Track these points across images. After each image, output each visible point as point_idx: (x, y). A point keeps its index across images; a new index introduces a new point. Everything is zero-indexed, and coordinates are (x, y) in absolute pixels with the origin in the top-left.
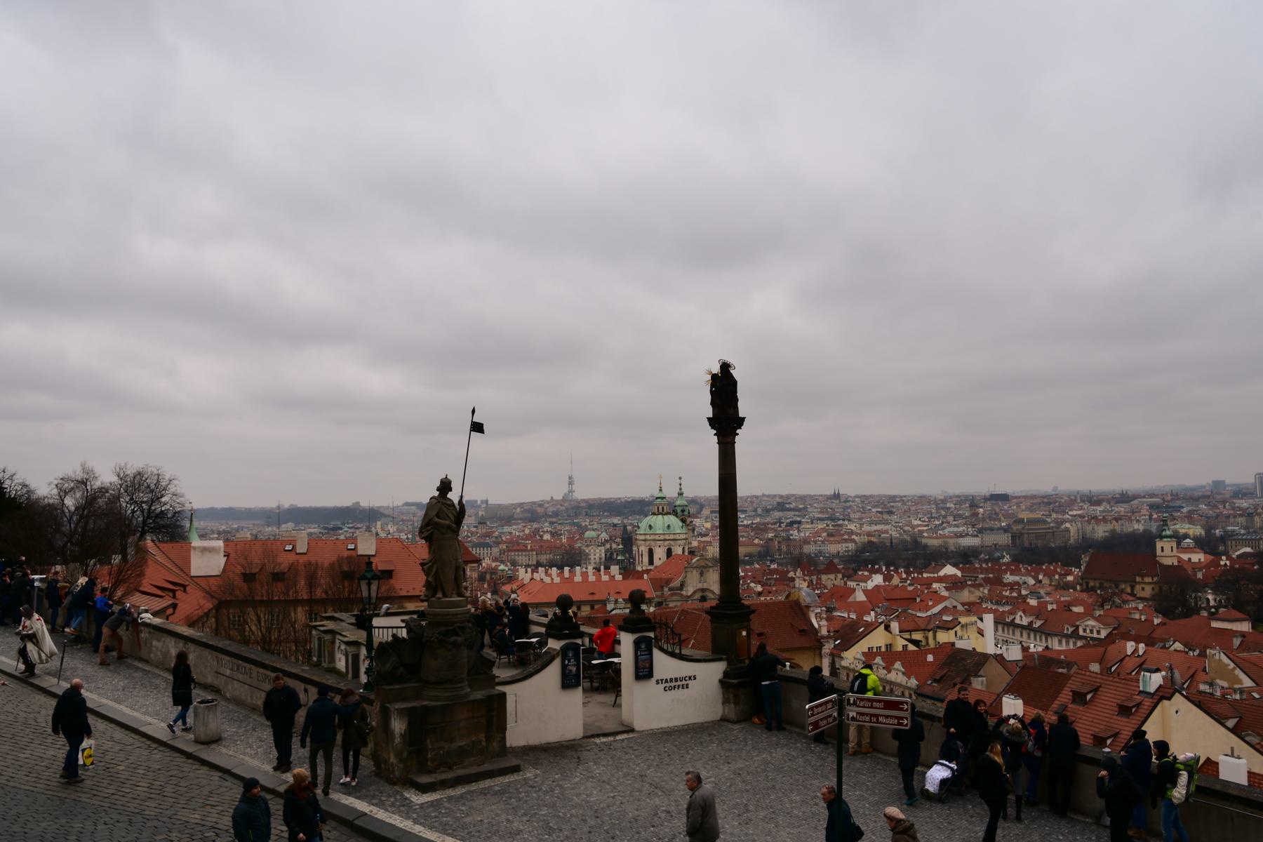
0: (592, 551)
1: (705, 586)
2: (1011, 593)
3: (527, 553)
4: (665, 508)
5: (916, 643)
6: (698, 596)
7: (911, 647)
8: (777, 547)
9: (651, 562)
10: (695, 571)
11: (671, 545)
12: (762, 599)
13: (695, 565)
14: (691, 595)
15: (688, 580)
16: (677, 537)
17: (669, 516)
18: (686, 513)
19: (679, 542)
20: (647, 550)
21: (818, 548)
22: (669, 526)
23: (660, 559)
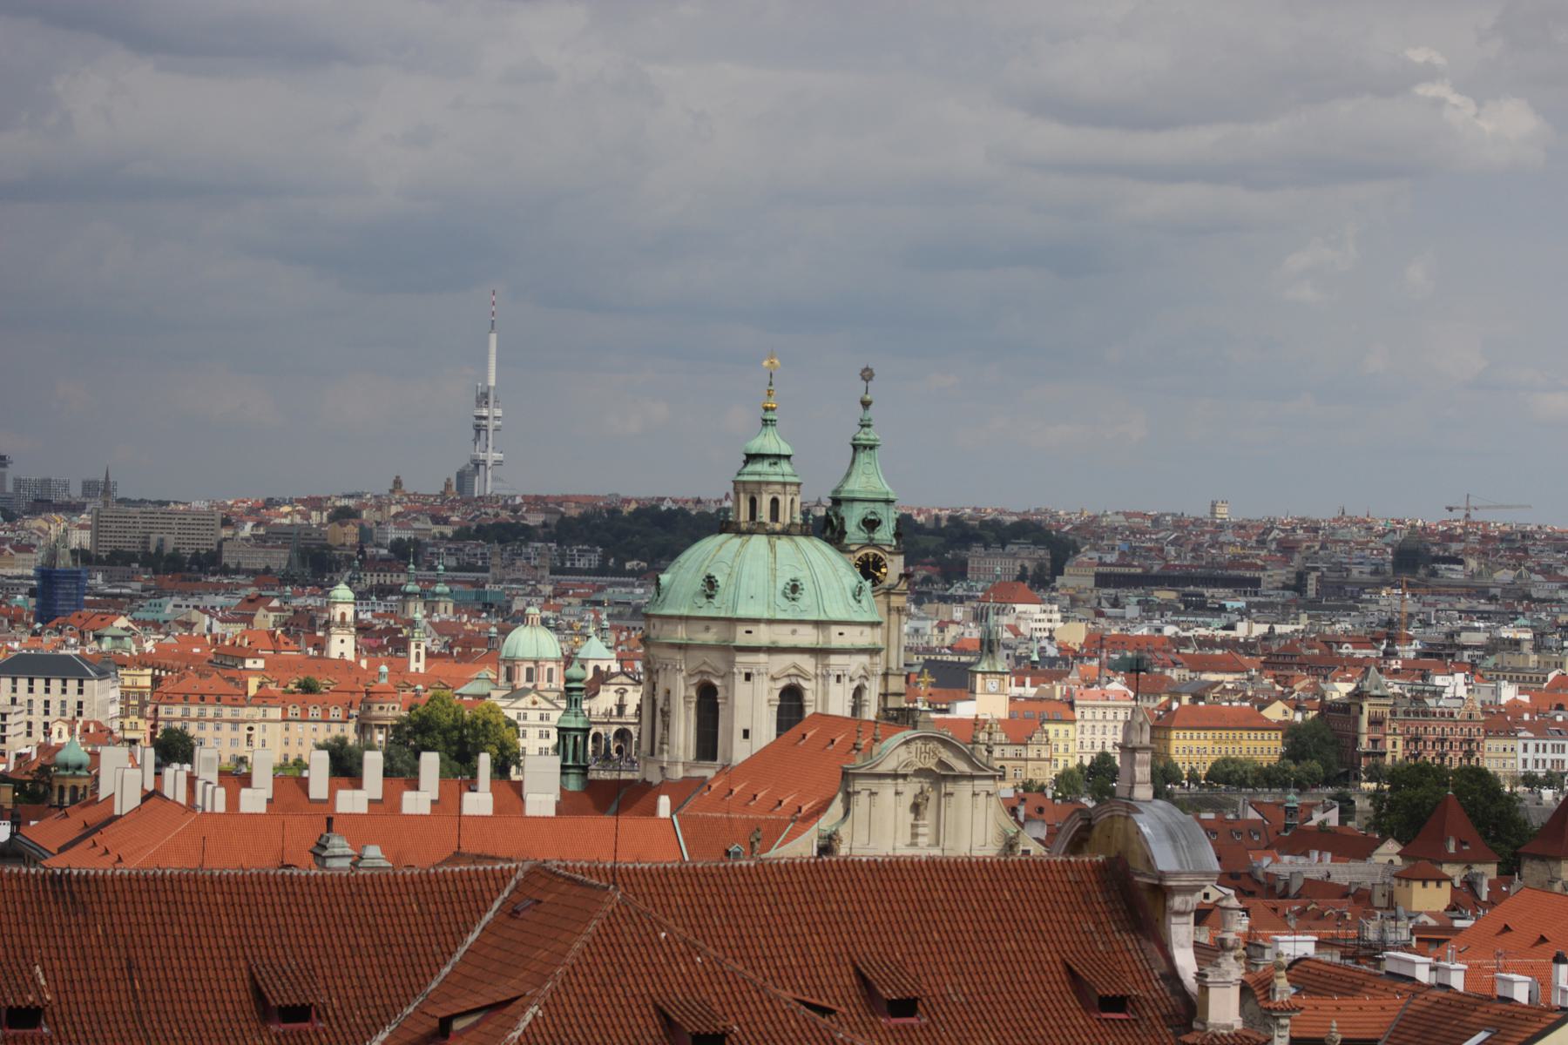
0: (533, 716)
3: (245, 713)
4: (784, 502)
9: (707, 745)
11: (802, 674)
16: (835, 639)
21: (1549, 756)
22: (795, 587)
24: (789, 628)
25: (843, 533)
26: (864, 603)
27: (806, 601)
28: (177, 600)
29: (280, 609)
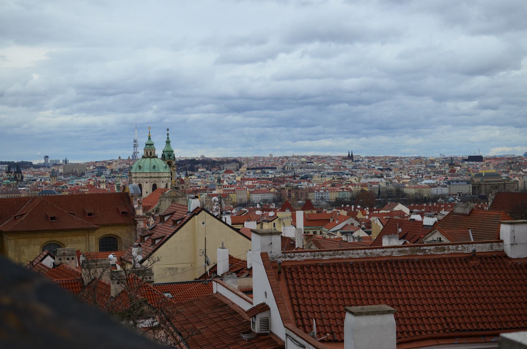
16: (161, 175)
19: (162, 179)
22: (154, 167)
23: (147, 192)
24: (153, 174)
25: (165, 157)
26: (167, 169)
27: (156, 169)
28: (76, 180)
29: (95, 181)
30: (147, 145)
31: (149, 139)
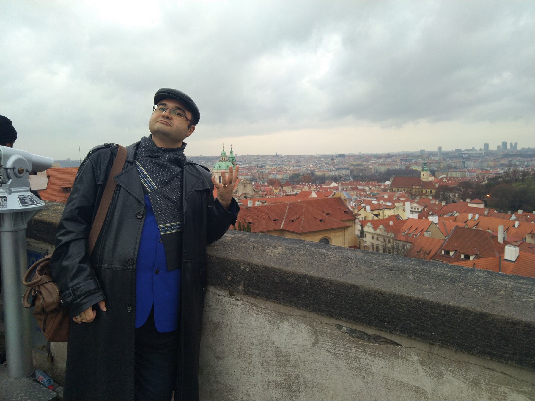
1: (246, 192)
2: (363, 193)
4: (226, 158)
5: (377, 215)
6: (243, 196)
7: (375, 218)
8: (258, 176)
10: (242, 186)
12: (267, 197)
13: (242, 183)
14: (241, 196)
15: (239, 189)
17: (228, 162)
18: (234, 161)
20: (218, 177)
25: (230, 161)
30: (222, 154)
31: (224, 150)
